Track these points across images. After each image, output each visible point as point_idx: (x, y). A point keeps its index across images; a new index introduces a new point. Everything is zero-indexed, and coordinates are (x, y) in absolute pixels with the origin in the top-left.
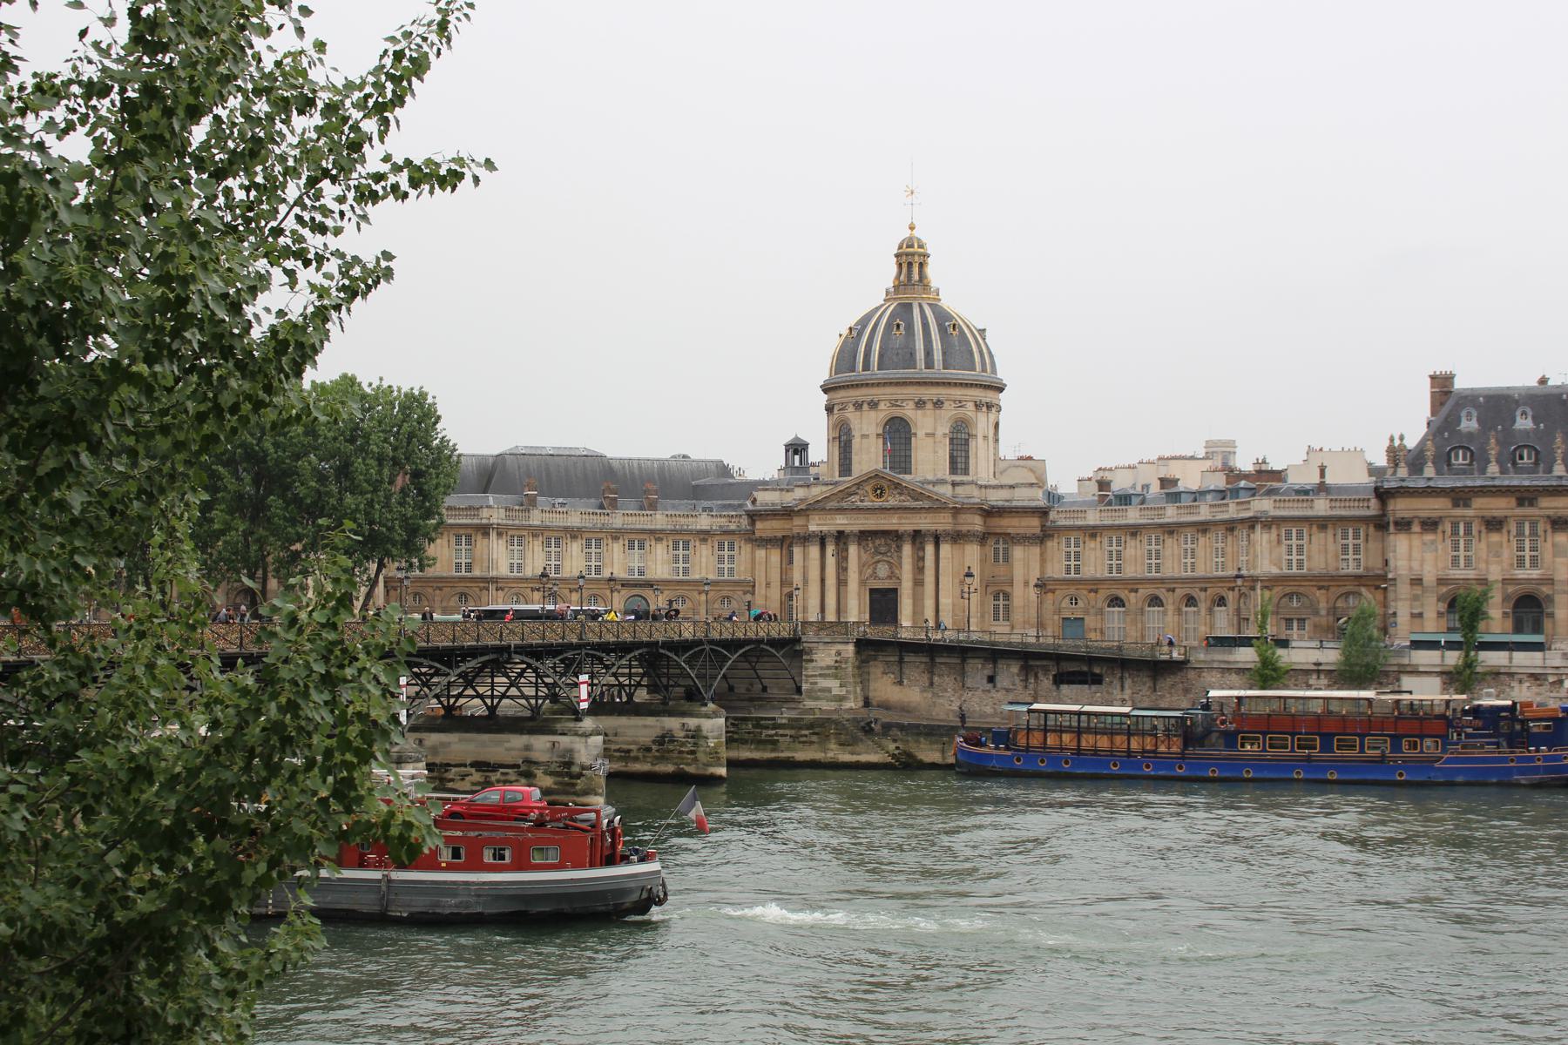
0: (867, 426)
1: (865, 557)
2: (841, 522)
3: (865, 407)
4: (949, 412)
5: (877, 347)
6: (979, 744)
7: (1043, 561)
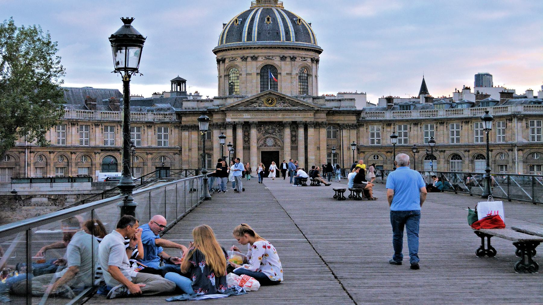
1: (259, 135)
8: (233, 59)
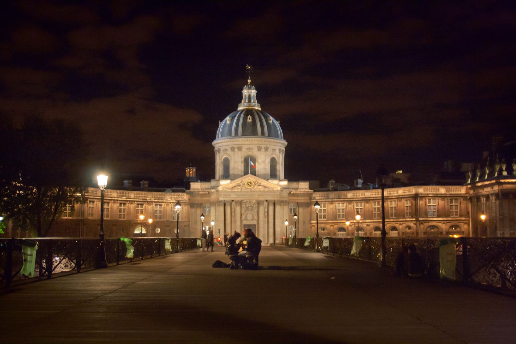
3: (236, 150)
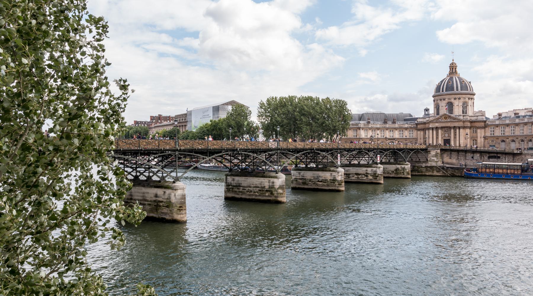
0: (443, 105)
2: (437, 125)
4: (462, 100)
5: (445, 87)
6: (470, 171)
7: (485, 132)
8: (437, 100)
